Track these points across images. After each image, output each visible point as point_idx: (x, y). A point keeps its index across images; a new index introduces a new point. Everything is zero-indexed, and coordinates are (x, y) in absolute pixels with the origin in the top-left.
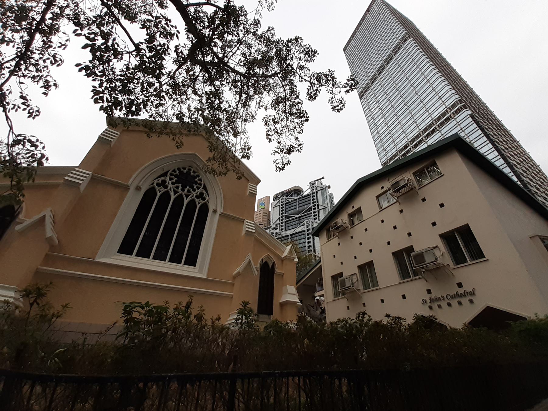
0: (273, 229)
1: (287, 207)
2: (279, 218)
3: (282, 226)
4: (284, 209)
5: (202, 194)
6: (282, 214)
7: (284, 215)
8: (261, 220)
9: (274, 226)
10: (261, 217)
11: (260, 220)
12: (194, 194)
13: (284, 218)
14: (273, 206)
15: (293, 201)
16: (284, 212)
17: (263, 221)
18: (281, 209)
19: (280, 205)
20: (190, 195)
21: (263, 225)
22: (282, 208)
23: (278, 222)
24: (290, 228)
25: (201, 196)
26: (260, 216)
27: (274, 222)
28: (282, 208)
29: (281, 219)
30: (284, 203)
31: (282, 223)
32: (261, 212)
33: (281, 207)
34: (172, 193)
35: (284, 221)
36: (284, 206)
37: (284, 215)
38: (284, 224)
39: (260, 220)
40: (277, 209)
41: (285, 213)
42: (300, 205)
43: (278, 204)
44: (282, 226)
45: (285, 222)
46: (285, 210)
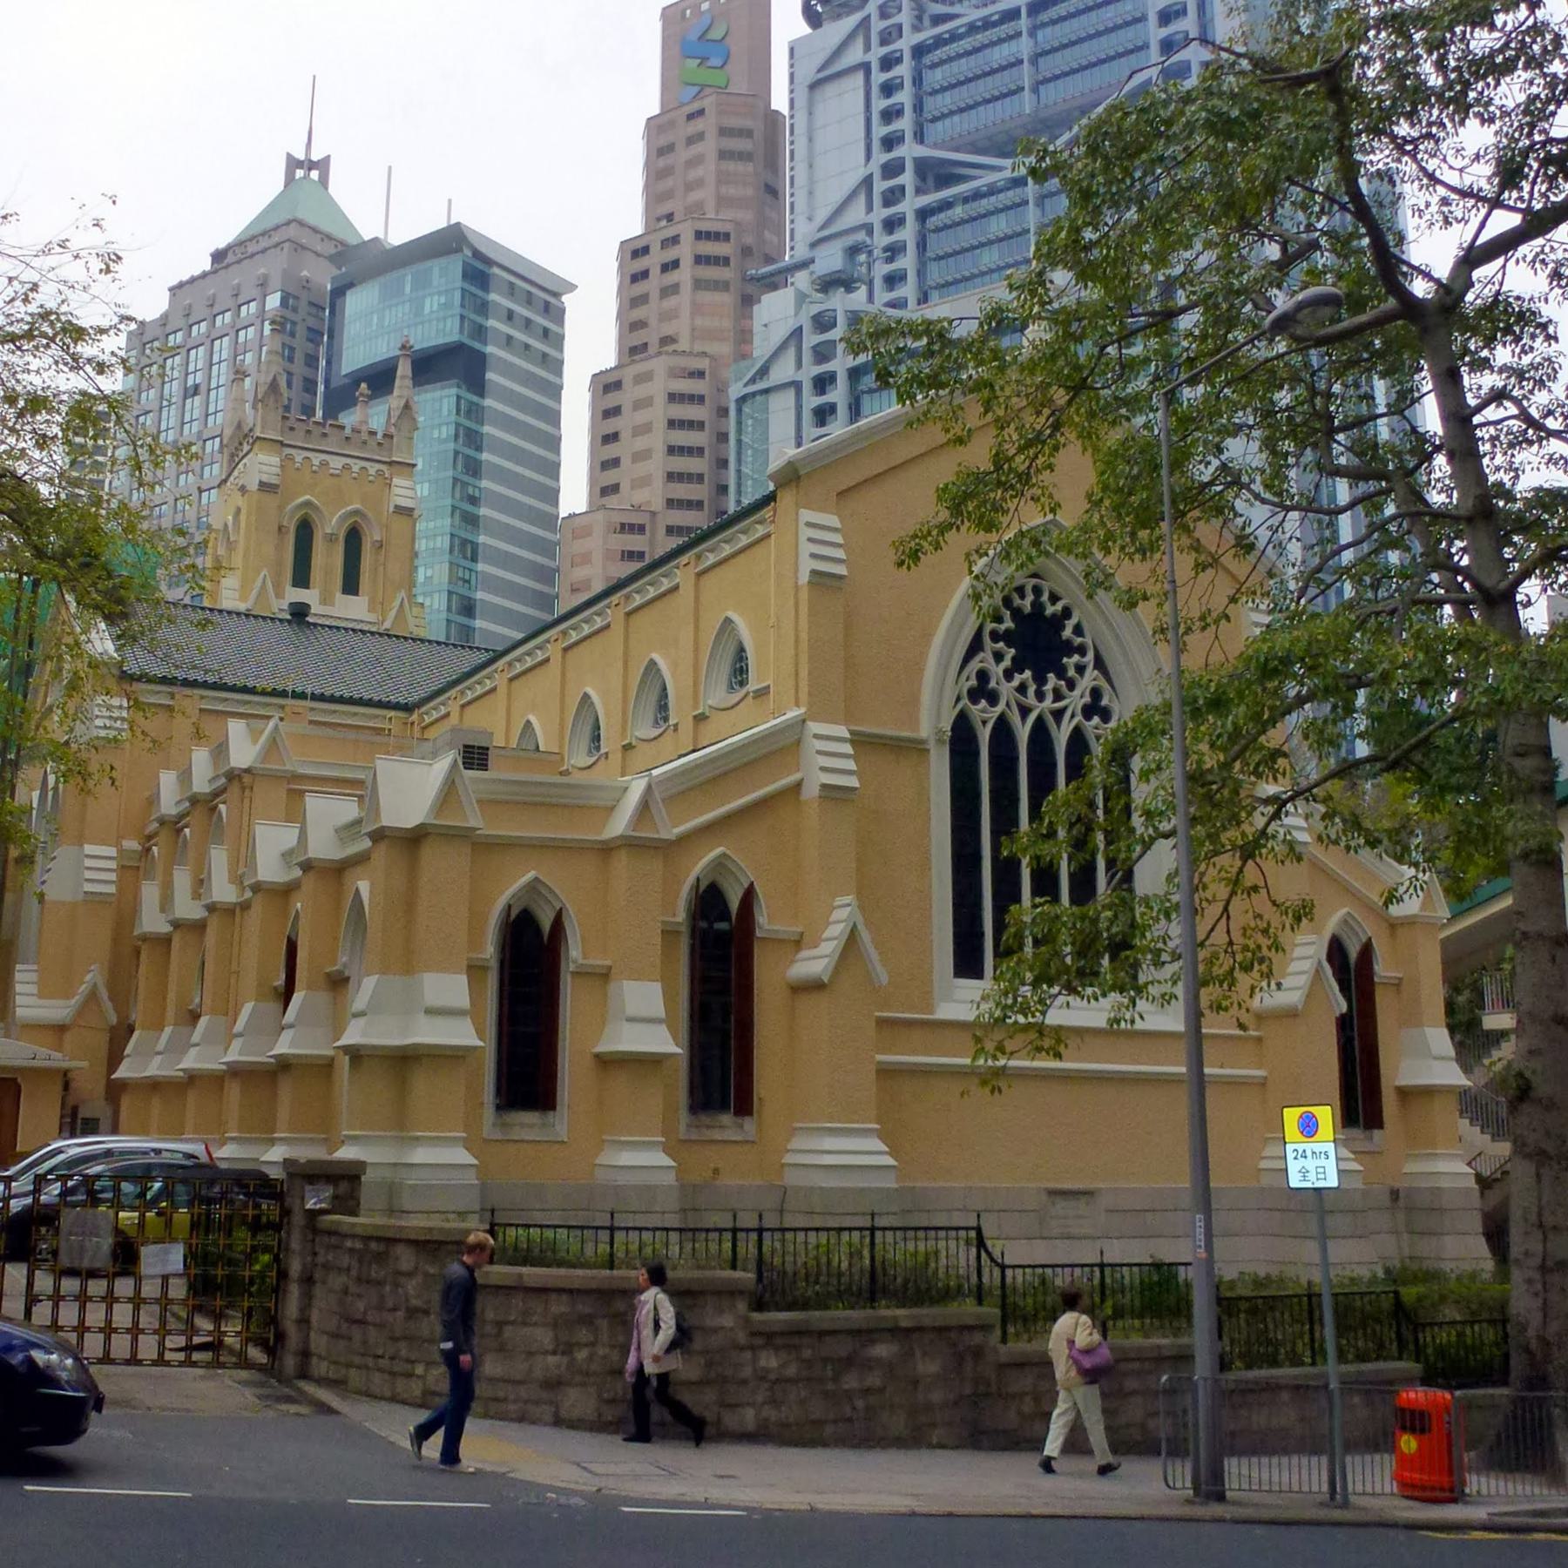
0: (828, 284)
1: (936, 77)
2: (868, 182)
3: (894, 251)
4: (904, 97)
5: (1096, 693)
6: (889, 143)
7: (909, 151)
8: (706, 195)
9: (831, 259)
10: (708, 170)
11: (695, 196)
12: (1077, 699)
13: (907, 178)
14: (808, 73)
15: (987, 24)
16: (905, 124)
17: (723, 202)
18: (879, 104)
19: (866, 67)
20: (1065, 708)
21: (727, 237)
22: (888, 89)
23: (856, 214)
24: (965, 266)
25: (1095, 708)
26: (696, 161)
27: (822, 215)
28: (888, 89)
29: (880, 186)
30: (905, 44)
31: (891, 225)
32: (699, 125)
33: (879, 77)
34: (1015, 717)
35: (909, 206)
36: (904, 70)
37: (909, 151)
38: (907, 234)
39: (695, 196)
40: (847, 99)
41: (920, 137)
42: (1050, 65)
43: (855, 55)
44: (894, 251)
45: (923, 214)
46: (918, 107)
